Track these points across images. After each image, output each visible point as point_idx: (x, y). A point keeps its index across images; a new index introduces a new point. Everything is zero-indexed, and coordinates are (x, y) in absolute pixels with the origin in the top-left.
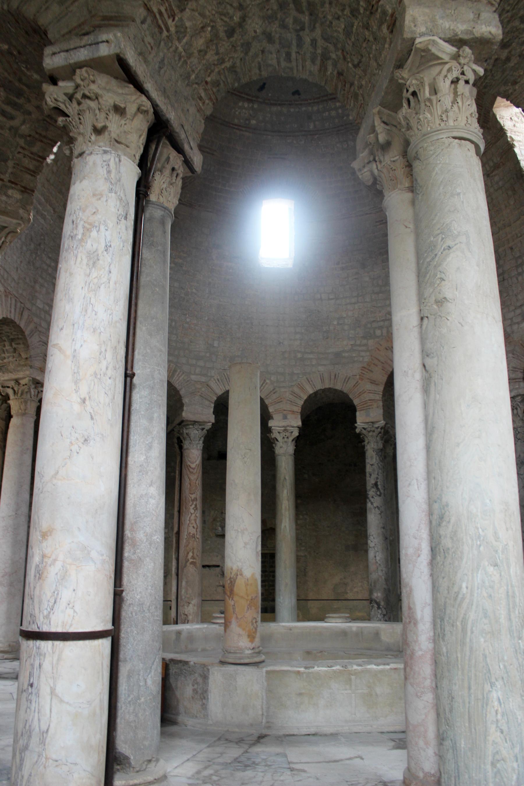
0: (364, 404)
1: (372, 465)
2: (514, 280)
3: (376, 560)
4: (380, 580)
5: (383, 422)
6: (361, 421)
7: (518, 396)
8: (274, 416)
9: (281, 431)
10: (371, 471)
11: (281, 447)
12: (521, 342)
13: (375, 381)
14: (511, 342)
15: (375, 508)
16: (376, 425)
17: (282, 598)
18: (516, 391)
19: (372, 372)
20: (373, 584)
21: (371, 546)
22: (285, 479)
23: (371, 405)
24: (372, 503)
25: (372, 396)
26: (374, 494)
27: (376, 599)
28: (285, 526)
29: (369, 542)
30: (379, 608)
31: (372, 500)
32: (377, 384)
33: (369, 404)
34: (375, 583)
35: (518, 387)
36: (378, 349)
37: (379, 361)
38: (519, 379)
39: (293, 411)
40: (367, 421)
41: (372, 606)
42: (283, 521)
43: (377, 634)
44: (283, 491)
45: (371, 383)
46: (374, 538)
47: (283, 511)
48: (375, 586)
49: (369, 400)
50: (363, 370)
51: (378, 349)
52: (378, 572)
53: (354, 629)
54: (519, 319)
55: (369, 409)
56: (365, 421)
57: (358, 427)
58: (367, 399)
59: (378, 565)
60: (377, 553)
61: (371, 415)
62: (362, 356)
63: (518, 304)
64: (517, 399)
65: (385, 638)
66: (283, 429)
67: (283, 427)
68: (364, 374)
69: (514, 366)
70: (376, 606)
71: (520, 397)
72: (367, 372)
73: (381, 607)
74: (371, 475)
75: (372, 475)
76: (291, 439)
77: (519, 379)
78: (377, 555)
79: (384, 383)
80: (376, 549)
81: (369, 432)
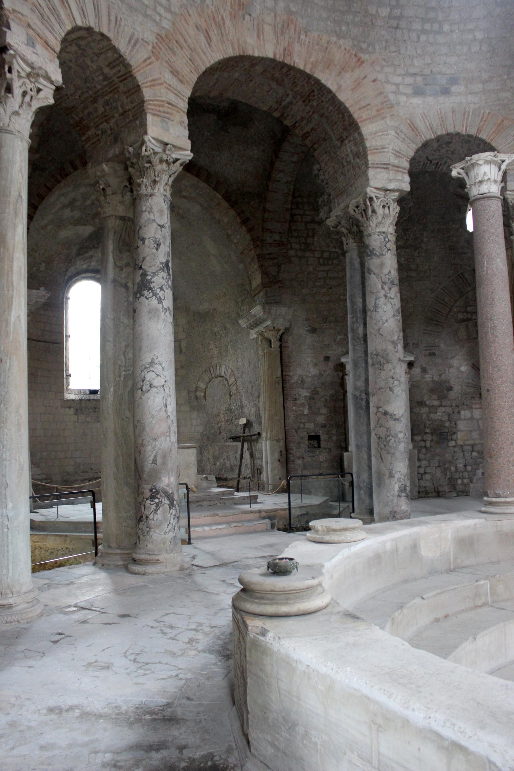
0: (159, 106)
1: (162, 226)
2: (414, 36)
3: (166, 411)
4: (173, 449)
5: (189, 152)
6: (154, 136)
7: (397, 190)
8: (13, 24)
9: (23, 74)
10: (158, 236)
11: (16, 113)
12: (408, 121)
13: (177, 72)
14: (394, 115)
15: (166, 310)
16: (174, 156)
17: (10, 505)
18: (398, 184)
19: (174, 53)
20: (159, 461)
21: (155, 383)
22: (20, 196)
23: (171, 114)
24: (160, 300)
25: (172, 97)
26: (163, 282)
27: (167, 488)
28: (19, 317)
29: (150, 376)
30: (171, 505)
31: (161, 294)
32: (181, 82)
33: (166, 109)
34: (164, 457)
35: (401, 178)
36: (185, 19)
37: (186, 43)
38: (404, 169)
39: (46, 43)
40: (166, 140)
41: (157, 504)
42: (15, 303)
43: (414, 547)
44: (15, 226)
45: (172, 72)
46: (163, 369)
47: (15, 278)
48: (164, 463)
49: (168, 103)
50: (161, 43)
51: (185, 19)
52: (170, 436)
53: (388, 546)
54: (409, 91)
55: (168, 119)
56: (161, 138)
57: (148, 144)
58: (164, 99)
59: (170, 421)
60: (169, 399)
61: (170, 131)
62: (160, 15)
63: (412, 71)
64: (393, 194)
65: (428, 552)
66: (28, 70)
67: (31, 66)
68: (160, 49)
69: (397, 149)
70: (167, 502)
71: (397, 194)
72: (167, 50)
73: (175, 502)
74: (159, 245)
75: (162, 245)
76: (36, 105)
77: (404, 169)
78: (168, 403)
79: (193, 85)
80: (167, 390)
81: (161, 161)
